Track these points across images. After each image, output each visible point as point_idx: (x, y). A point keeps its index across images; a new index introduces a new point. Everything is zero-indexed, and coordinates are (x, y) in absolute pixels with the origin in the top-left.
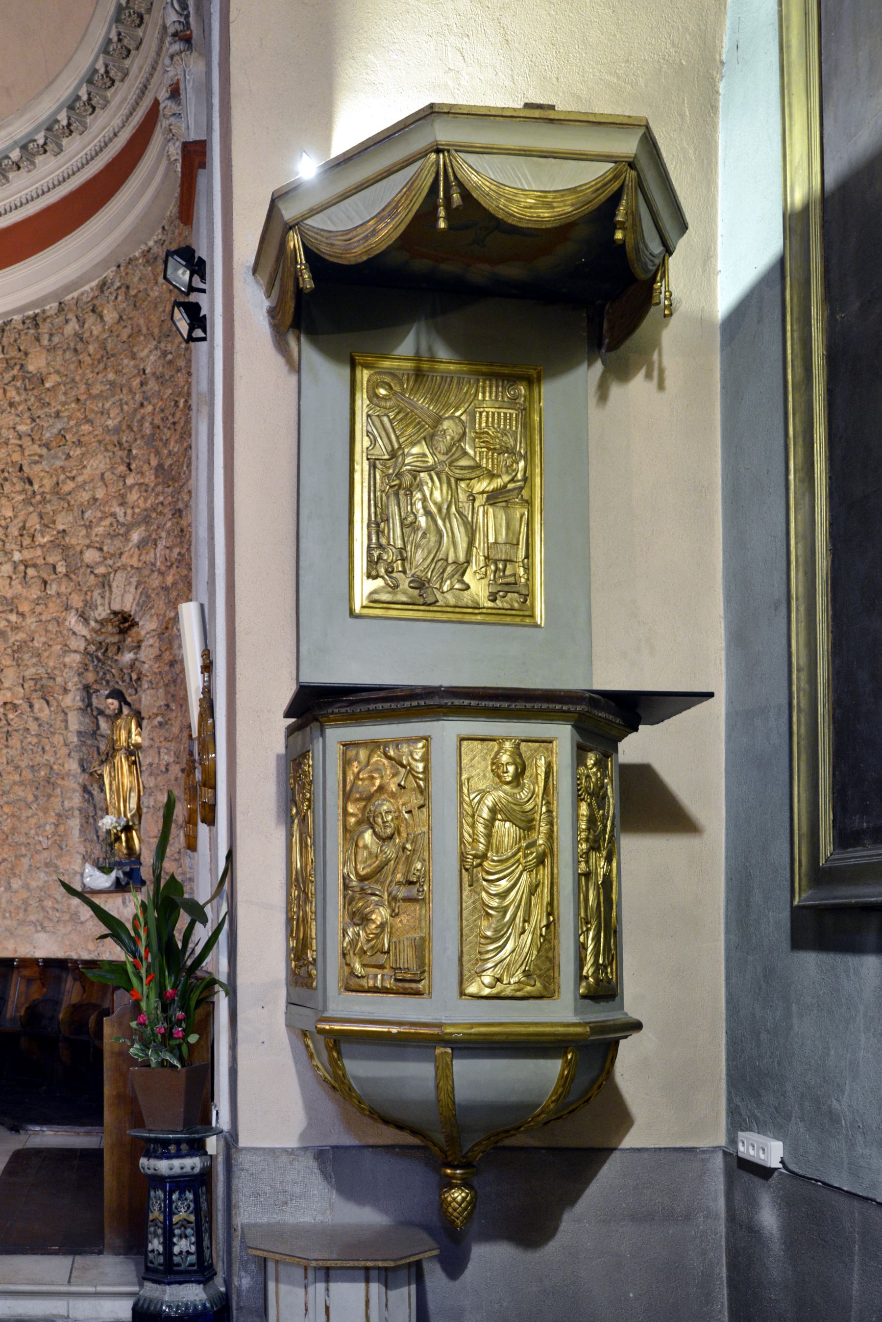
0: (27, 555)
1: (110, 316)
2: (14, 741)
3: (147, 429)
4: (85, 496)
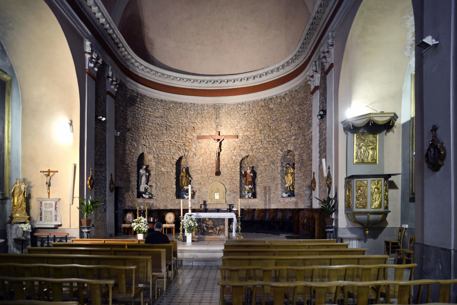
0: (269, 139)
1: (287, 99)
2: (267, 172)
3: (296, 120)
4: (282, 130)
